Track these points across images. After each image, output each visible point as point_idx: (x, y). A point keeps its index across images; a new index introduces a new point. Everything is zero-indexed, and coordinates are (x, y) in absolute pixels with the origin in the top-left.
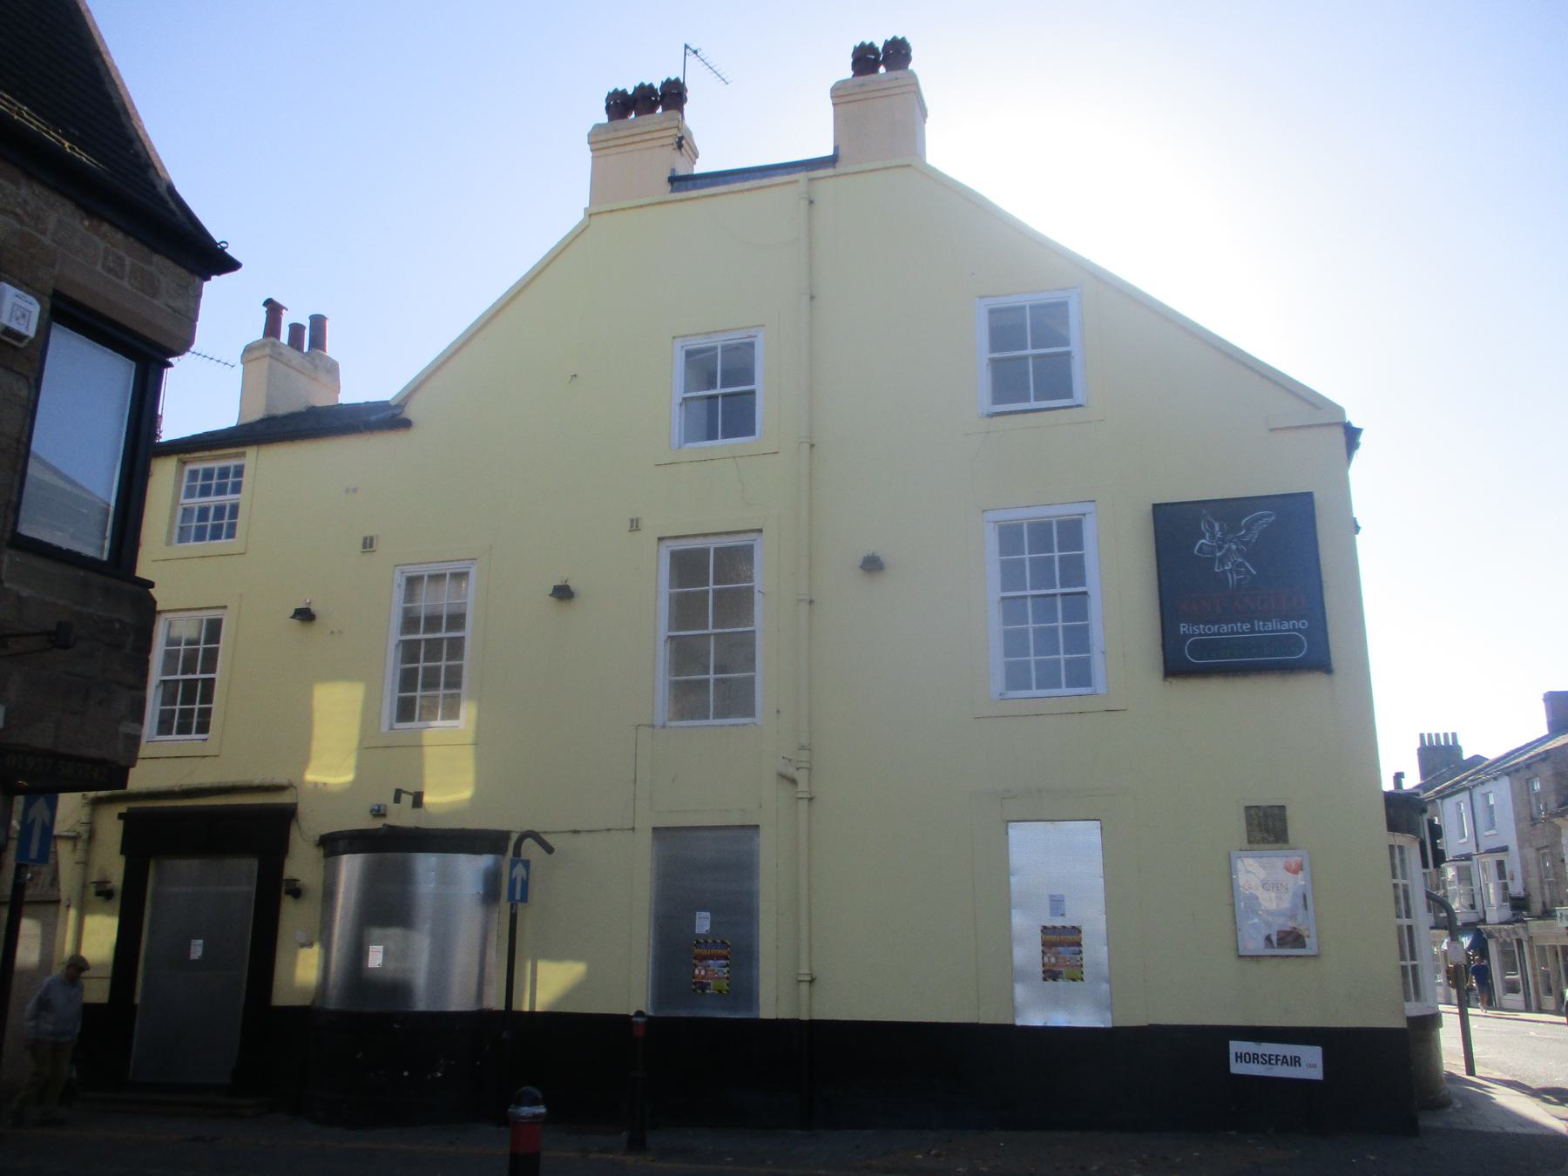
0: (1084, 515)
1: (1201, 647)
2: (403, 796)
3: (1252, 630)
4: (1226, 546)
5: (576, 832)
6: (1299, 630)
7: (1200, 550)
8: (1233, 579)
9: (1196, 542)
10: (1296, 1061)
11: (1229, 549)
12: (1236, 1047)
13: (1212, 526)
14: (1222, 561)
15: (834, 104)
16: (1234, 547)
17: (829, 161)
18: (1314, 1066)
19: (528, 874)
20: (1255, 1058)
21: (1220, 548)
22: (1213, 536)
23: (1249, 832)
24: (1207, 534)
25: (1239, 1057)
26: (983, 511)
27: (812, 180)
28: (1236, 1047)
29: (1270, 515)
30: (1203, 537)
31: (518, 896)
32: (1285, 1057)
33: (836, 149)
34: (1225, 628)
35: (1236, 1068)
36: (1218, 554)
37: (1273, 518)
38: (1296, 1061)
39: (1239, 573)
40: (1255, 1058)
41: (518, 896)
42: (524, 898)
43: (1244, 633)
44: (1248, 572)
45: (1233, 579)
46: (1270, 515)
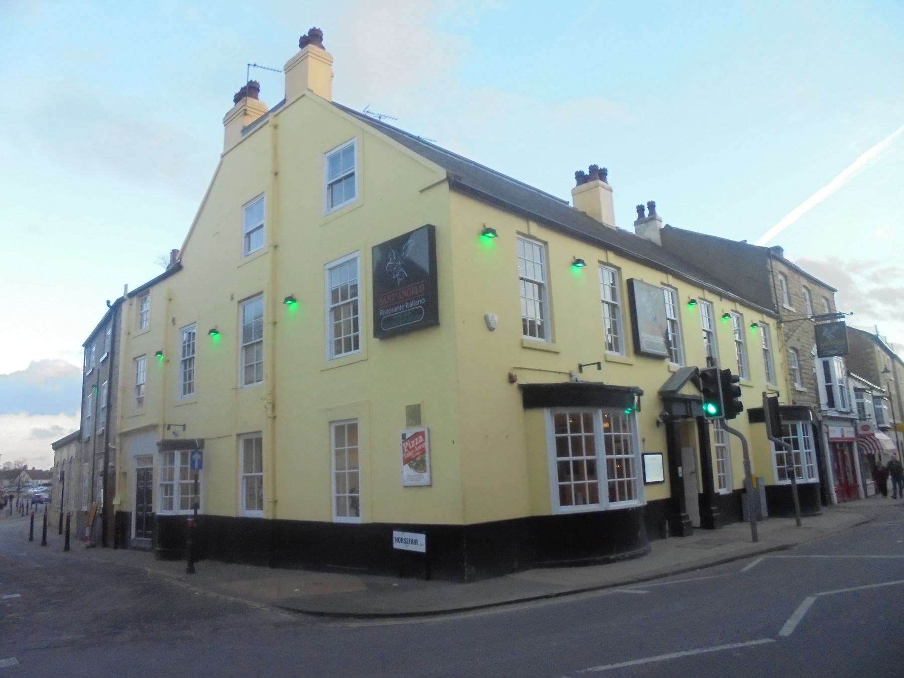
0: (356, 258)
1: (390, 320)
2: (171, 427)
3: (405, 308)
4: (397, 263)
5: (219, 438)
6: (420, 305)
7: (388, 269)
8: (399, 280)
9: (387, 263)
10: (415, 542)
11: (398, 265)
12: (396, 534)
13: (392, 254)
14: (396, 274)
15: (285, 73)
16: (400, 263)
17: (284, 102)
18: (422, 545)
19: (202, 457)
20: (401, 540)
21: (395, 265)
22: (392, 257)
23: (407, 419)
24: (391, 259)
25: (398, 540)
26: (325, 265)
27: (276, 116)
28: (396, 534)
29: (413, 242)
30: (389, 261)
31: (196, 466)
32: (412, 540)
33: (286, 95)
34: (396, 309)
35: (397, 545)
36: (395, 269)
37: (414, 243)
38: (415, 542)
39: (401, 277)
40: (401, 540)
41: (196, 466)
42: (200, 467)
43: (402, 310)
44: (405, 276)
45: (399, 280)
46: (413, 242)
